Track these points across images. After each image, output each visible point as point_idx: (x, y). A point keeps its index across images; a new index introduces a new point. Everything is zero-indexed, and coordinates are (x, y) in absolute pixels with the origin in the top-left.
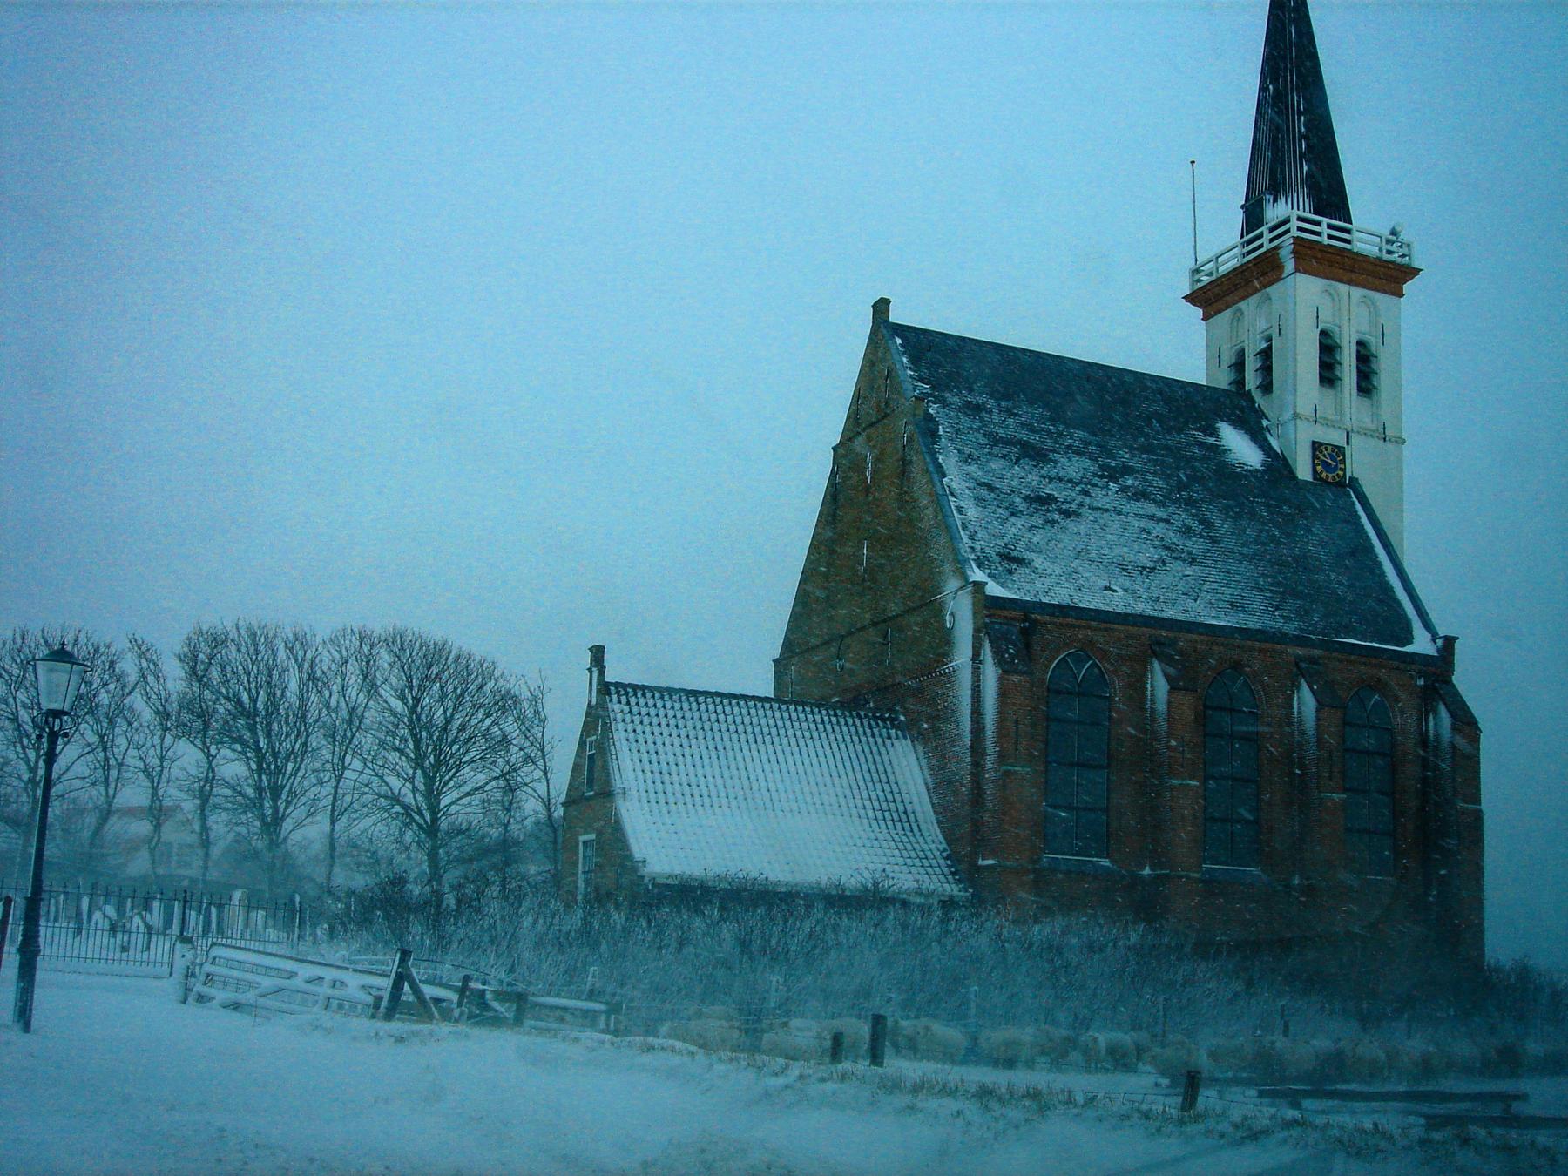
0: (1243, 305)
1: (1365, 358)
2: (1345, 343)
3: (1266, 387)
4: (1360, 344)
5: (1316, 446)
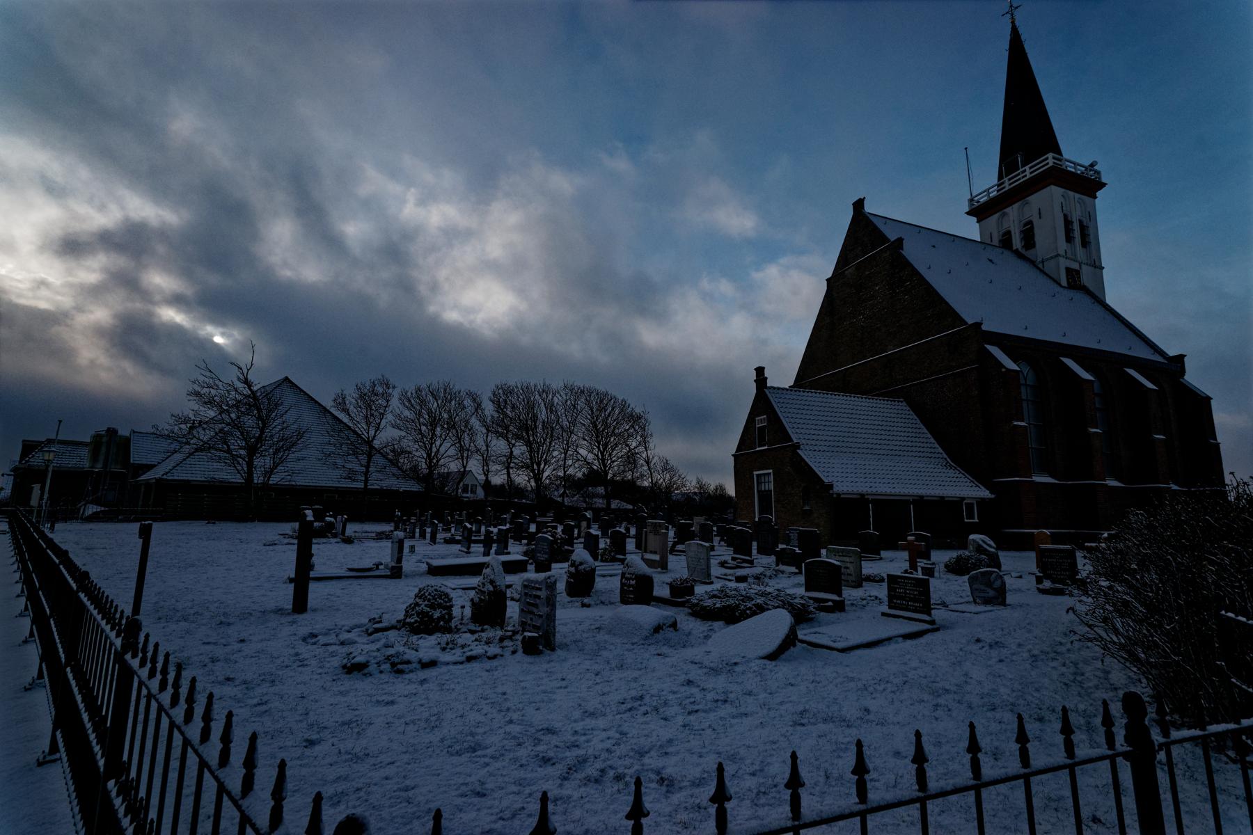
0: (1008, 210)
2: (1074, 220)
4: (1081, 222)
5: (1068, 270)
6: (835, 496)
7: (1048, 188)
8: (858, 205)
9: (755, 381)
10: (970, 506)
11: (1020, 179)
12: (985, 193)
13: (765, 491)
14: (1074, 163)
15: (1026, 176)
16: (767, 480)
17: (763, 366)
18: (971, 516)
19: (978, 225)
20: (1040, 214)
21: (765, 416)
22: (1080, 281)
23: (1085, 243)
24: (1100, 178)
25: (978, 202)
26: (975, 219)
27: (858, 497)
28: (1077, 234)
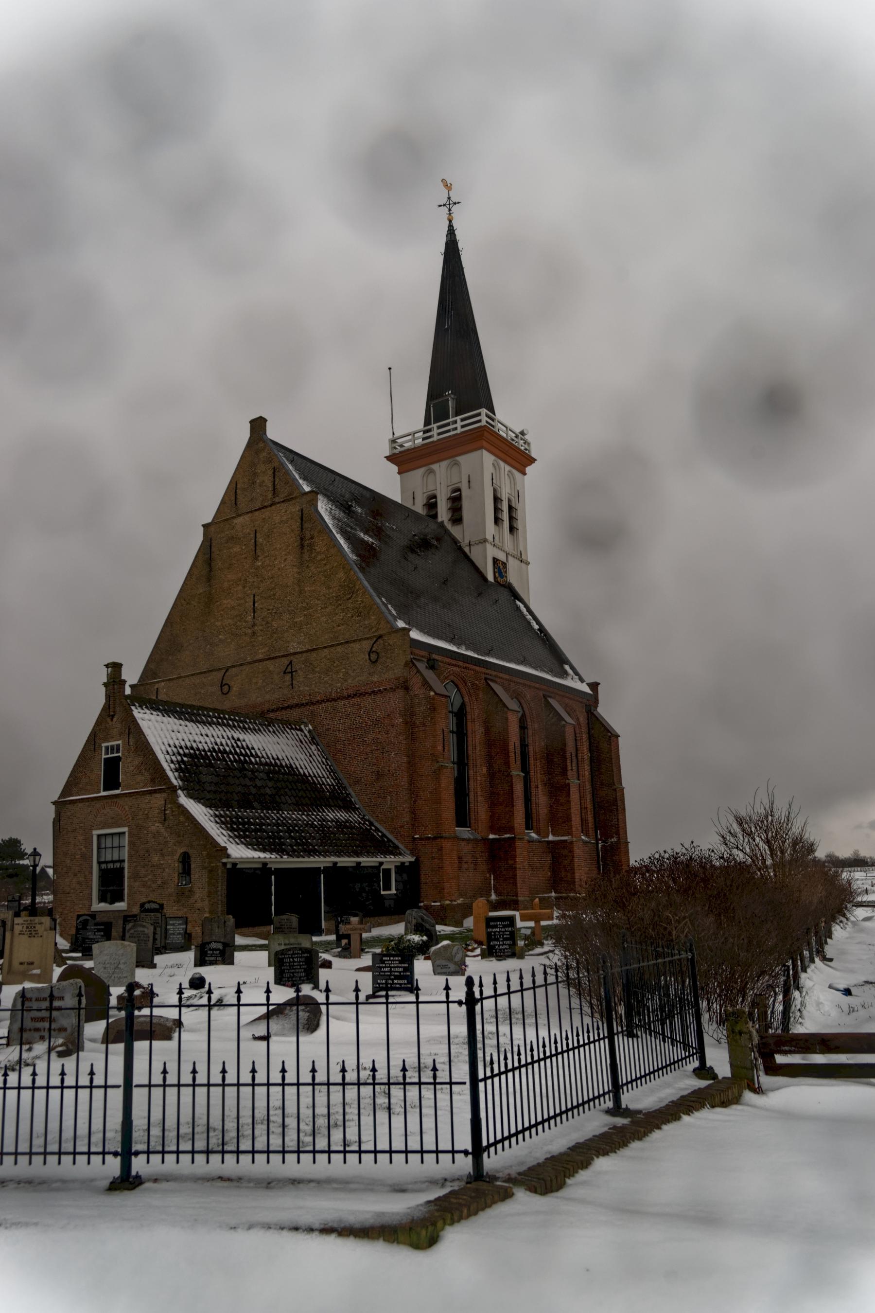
0: (435, 467)
1: (511, 508)
2: (503, 498)
3: (457, 519)
4: (509, 500)
5: (495, 561)
6: (229, 866)
7: (478, 453)
8: (258, 425)
9: (105, 684)
10: (387, 872)
11: (449, 431)
12: (410, 437)
13: (113, 862)
14: (507, 428)
15: (456, 429)
16: (116, 844)
17: (119, 661)
18: (387, 887)
19: (398, 476)
20: (469, 482)
21: (120, 742)
22: (506, 577)
23: (512, 529)
24: (529, 451)
25: (401, 446)
26: (395, 468)
27: (260, 866)
28: (505, 516)
